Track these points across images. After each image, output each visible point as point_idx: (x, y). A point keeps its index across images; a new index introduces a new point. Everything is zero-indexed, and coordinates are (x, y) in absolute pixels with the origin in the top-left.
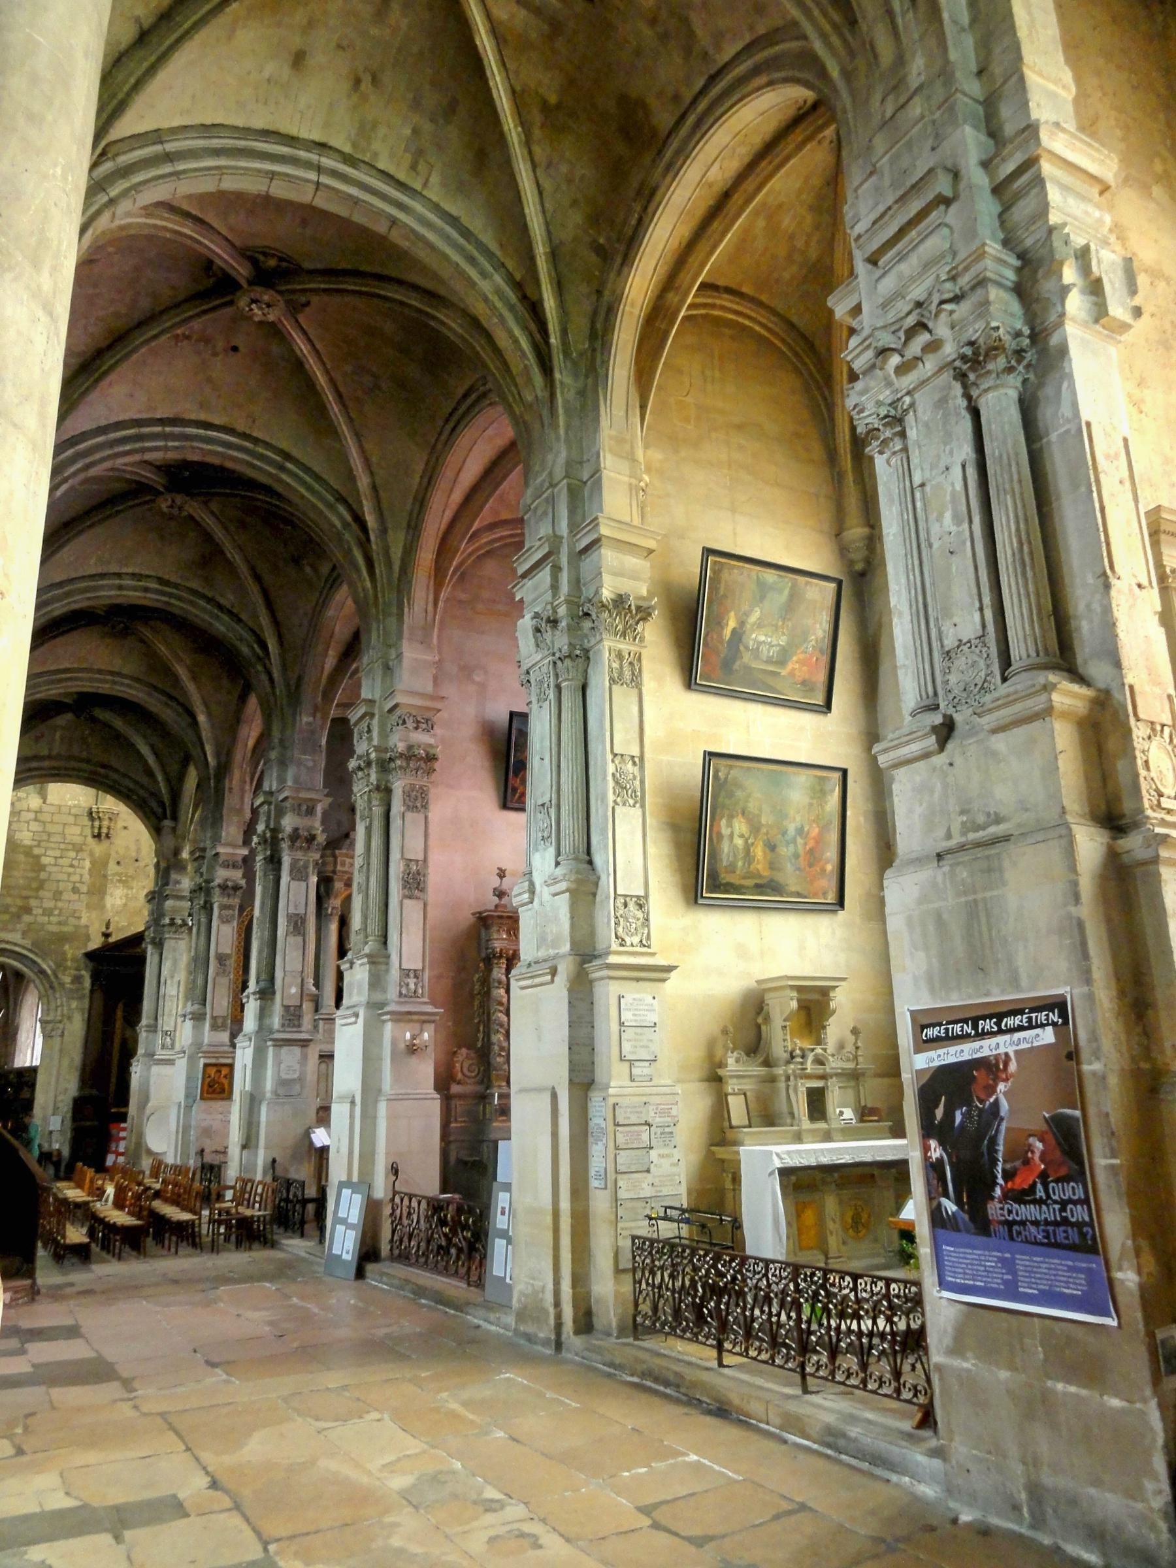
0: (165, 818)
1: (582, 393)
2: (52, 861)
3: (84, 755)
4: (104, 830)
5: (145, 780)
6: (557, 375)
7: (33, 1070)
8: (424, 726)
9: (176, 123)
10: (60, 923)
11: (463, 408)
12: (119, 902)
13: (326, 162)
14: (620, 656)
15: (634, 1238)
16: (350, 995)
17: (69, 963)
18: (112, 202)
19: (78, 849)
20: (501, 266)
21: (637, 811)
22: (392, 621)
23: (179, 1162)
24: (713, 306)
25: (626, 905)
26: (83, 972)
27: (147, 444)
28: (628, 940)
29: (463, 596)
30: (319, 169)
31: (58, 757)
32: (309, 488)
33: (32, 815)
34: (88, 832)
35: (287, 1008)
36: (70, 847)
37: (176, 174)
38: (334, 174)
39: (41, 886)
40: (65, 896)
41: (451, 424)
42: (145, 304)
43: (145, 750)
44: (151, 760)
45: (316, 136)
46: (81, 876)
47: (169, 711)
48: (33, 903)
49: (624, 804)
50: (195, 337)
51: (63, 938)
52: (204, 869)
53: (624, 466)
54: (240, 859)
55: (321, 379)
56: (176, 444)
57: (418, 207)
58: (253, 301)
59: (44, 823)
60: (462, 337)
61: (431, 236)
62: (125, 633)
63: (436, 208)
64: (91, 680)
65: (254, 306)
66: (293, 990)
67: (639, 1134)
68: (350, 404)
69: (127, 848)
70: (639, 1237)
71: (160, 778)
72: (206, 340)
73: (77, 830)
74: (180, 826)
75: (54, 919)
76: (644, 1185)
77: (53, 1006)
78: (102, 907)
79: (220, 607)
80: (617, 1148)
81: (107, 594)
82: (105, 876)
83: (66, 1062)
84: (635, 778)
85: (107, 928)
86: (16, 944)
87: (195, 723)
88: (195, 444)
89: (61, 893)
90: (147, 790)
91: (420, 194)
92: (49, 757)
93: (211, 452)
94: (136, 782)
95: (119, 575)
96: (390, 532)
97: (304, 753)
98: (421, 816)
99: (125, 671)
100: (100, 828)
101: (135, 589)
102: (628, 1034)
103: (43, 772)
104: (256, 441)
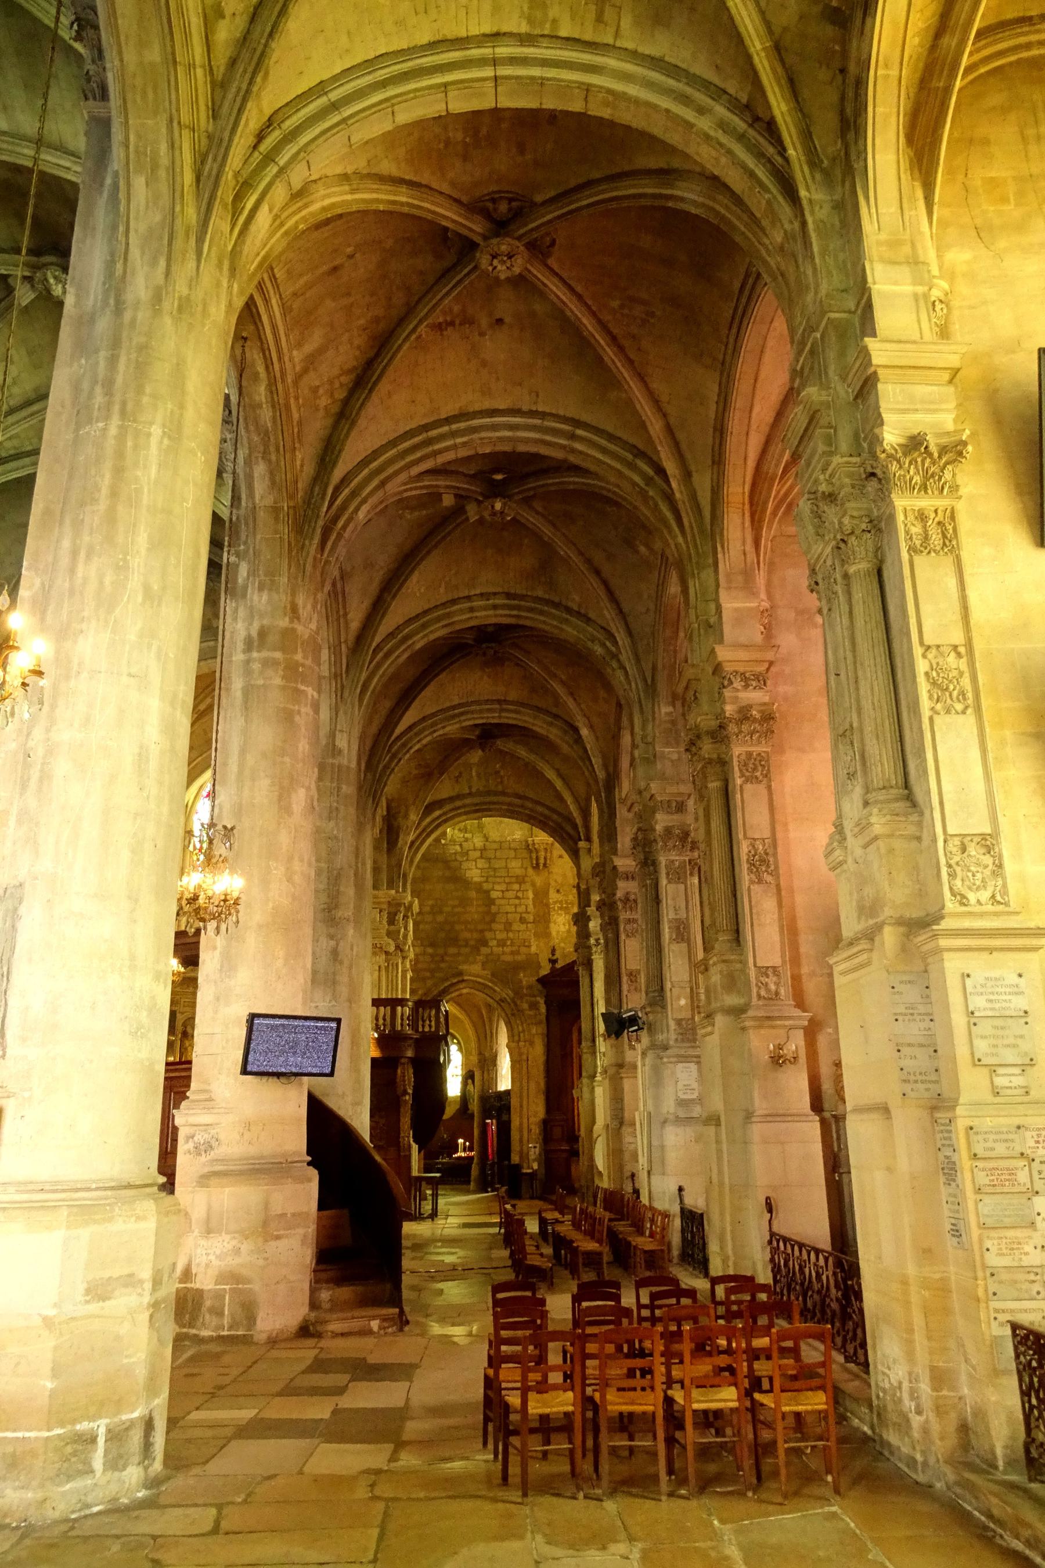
1: (839, 206)
2: (500, 894)
3: (500, 788)
4: (542, 861)
5: (556, 805)
6: (803, 193)
7: (507, 1093)
8: (754, 683)
9: (338, 70)
10: (512, 953)
11: (744, 300)
13: (502, 51)
14: (922, 516)
15: (1015, 1327)
18: (282, 170)
19: (521, 880)
20: (718, 93)
21: (970, 718)
22: (707, 574)
24: (1028, 46)
25: (964, 849)
27: (436, 447)
28: (972, 897)
30: (495, 62)
31: (479, 793)
32: (604, 450)
33: (478, 854)
34: (527, 863)
35: (679, 1022)
37: (344, 120)
38: (513, 61)
39: (493, 921)
40: (515, 927)
41: (734, 331)
42: (399, 299)
43: (550, 774)
44: (559, 784)
45: (487, 29)
48: (488, 935)
49: (948, 712)
50: (457, 322)
51: (517, 967)
52: (605, 884)
53: (904, 272)
55: (588, 323)
56: (464, 439)
57: (612, 62)
58: (494, 257)
60: (703, 205)
61: (633, 90)
62: (497, 661)
63: (634, 56)
64: (481, 711)
65: (495, 262)
66: (683, 1002)
67: (1012, 1172)
68: (626, 343)
69: (564, 876)
70: (1022, 1328)
71: (569, 800)
72: (468, 321)
75: (507, 950)
76: (1028, 1248)
77: (516, 1031)
78: (547, 935)
79: (568, 610)
80: (978, 1191)
81: (463, 619)
82: (547, 905)
84: (961, 674)
86: (478, 976)
87: (579, 740)
88: (483, 434)
89: (510, 924)
90: (559, 814)
91: (614, 46)
92: (470, 794)
93: (501, 439)
94: (548, 808)
95: (468, 598)
96: (695, 475)
97: (668, 744)
98: (762, 788)
99: (510, 698)
101: (485, 608)
102: (985, 1028)
104: (543, 415)
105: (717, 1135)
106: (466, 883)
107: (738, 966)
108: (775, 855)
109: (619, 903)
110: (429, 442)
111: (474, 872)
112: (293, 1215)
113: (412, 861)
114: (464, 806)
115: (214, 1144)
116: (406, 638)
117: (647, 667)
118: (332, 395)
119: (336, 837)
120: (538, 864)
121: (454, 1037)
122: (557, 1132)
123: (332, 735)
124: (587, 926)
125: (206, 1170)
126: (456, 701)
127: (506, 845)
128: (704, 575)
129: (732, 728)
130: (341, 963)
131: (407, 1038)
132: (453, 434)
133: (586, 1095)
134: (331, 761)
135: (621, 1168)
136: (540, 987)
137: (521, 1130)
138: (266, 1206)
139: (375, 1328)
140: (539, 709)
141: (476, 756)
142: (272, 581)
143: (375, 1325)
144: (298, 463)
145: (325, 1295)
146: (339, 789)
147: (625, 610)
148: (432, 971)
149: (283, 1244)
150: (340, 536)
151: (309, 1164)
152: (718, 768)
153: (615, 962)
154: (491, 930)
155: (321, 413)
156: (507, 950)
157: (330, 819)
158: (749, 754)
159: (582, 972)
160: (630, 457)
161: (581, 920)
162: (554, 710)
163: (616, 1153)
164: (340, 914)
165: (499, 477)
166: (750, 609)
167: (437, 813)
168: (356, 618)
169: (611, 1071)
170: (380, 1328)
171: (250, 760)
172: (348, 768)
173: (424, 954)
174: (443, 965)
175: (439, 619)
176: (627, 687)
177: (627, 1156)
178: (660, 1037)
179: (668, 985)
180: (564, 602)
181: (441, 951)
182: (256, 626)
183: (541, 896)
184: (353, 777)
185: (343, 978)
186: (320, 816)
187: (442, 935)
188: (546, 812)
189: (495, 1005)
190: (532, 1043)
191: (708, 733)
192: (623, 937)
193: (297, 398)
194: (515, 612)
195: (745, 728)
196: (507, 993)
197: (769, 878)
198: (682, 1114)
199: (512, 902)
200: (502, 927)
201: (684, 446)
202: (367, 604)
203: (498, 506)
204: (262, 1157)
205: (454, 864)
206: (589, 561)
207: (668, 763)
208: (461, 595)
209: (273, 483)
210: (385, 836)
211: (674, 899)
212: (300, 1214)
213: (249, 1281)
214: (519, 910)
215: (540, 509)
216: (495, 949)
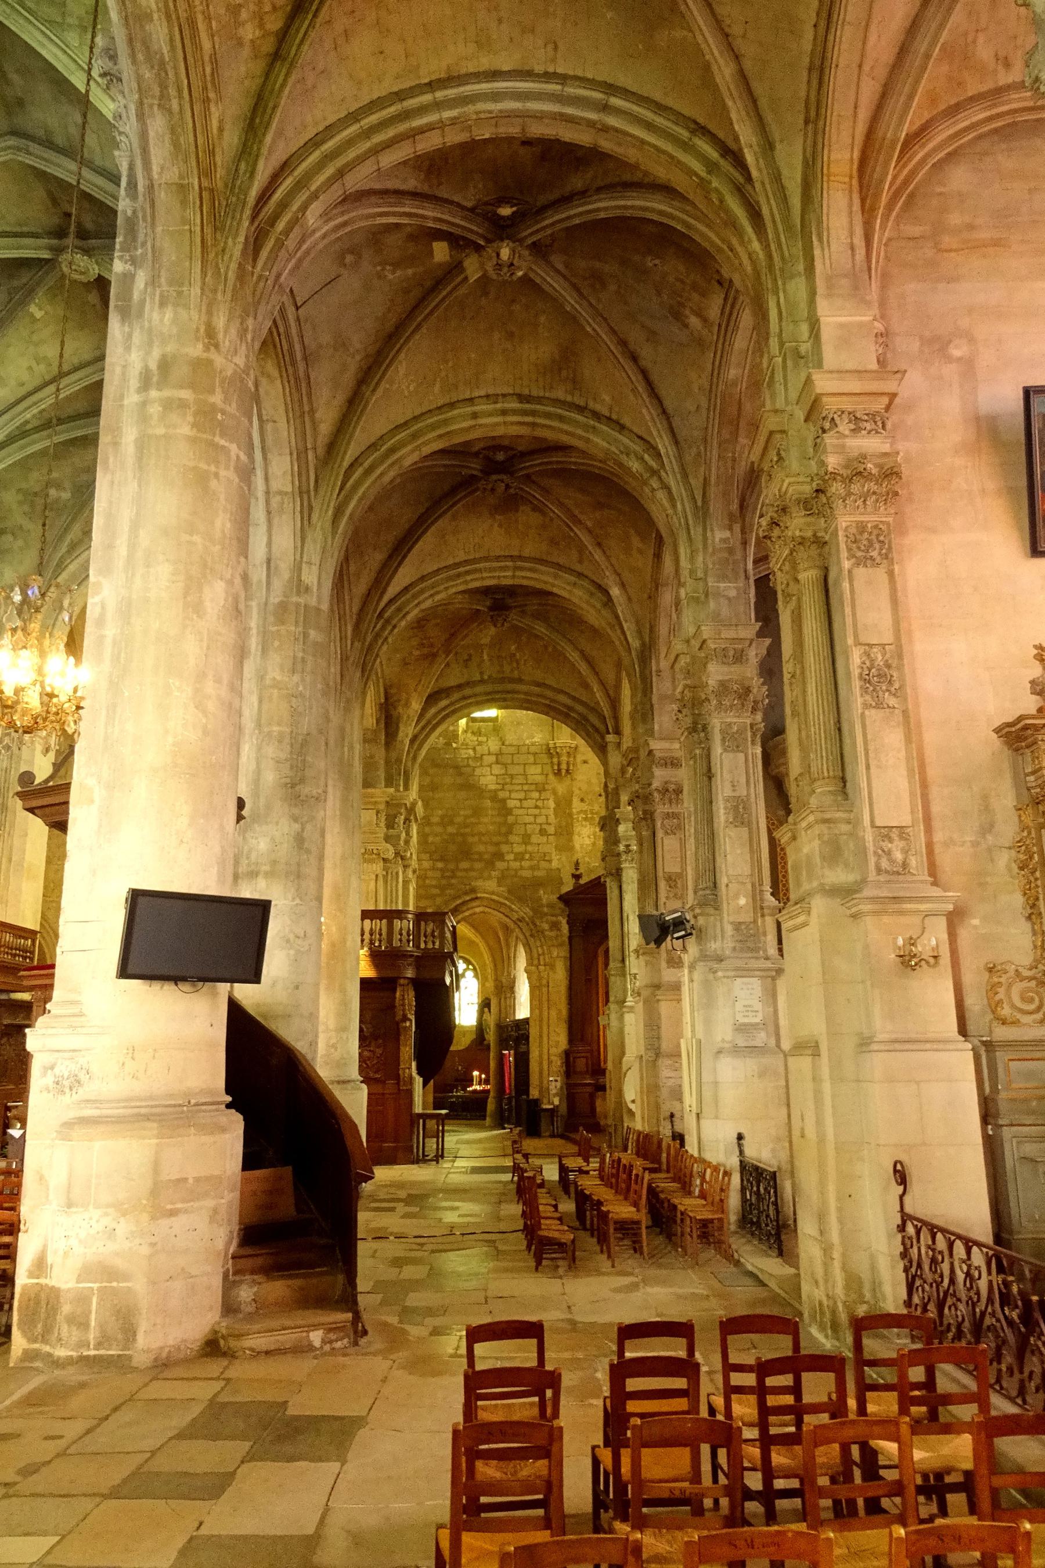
2: (518, 804)
3: (516, 674)
4: (564, 766)
7: (526, 1021)
10: (532, 868)
12: (587, 841)
16: (799, 884)
17: (545, 910)
19: (541, 788)
22: (798, 287)
23: (647, 1130)
26: (560, 918)
29: (916, 230)
31: (491, 680)
32: (649, 126)
33: (493, 759)
34: (548, 768)
35: (737, 926)
39: (510, 832)
40: (535, 839)
47: (578, 592)
48: (504, 848)
51: (537, 884)
62: (510, 503)
64: (491, 570)
66: (742, 901)
73: (538, 769)
75: (526, 864)
78: (569, 848)
79: (597, 416)
82: (570, 815)
83: (553, 1013)
86: (493, 893)
88: (481, 106)
89: (529, 836)
92: (482, 681)
94: (574, 698)
95: (471, 400)
96: (778, 146)
97: (723, 577)
98: (880, 574)
99: (526, 553)
103: (479, 699)
104: (563, 79)
105: (815, 1068)
107: (845, 828)
108: (900, 668)
109: (656, 794)
110: (406, 115)
111: (488, 778)
112: (197, 1180)
113: (415, 758)
115: (82, 1076)
116: (392, 450)
117: (696, 483)
118: (261, 26)
119: (301, 694)
120: (559, 770)
122: (581, 1064)
123: (297, 568)
124: (616, 831)
125: (73, 1114)
126: (461, 556)
127: (524, 749)
128: (791, 286)
129: (836, 488)
132: (438, 105)
133: (614, 1023)
136: (561, 905)
137: (541, 1063)
138: (156, 1167)
139: (317, 1343)
140: (559, 566)
141: (488, 633)
142: (180, 293)
143: (316, 1337)
144: (215, 124)
145: (245, 1293)
146: (306, 635)
147: (670, 410)
148: (443, 888)
149: (179, 1223)
150: (280, 244)
151: (229, 1106)
152: (814, 551)
153: (651, 863)
154: (507, 843)
155: (246, 52)
156: (526, 864)
157: (293, 671)
158: (862, 528)
159: (611, 886)
160: (684, 134)
161: (608, 824)
162: (578, 568)
163: (651, 1089)
164: (306, 790)
165: (506, 211)
166: (861, 325)
167: (444, 703)
168: (327, 417)
169: (645, 993)
170: (324, 1342)
171: (144, 538)
172: (318, 610)
173: (433, 869)
174: (453, 881)
175: (433, 427)
176: (670, 511)
177: (664, 1093)
178: (714, 946)
179: (723, 881)
180: (591, 405)
181: (452, 866)
182: (156, 353)
183: (563, 806)
184: (324, 622)
185: (311, 871)
186: (282, 669)
187: (453, 848)
188: (569, 702)
189: (512, 925)
190: (552, 967)
191: (798, 501)
192: (660, 834)
193: (208, 18)
194: (530, 419)
195: (855, 488)
196: (526, 912)
197: (892, 701)
198: (741, 1042)
199: (530, 811)
201: (763, 103)
202: (341, 398)
203: (505, 253)
204: (151, 1098)
205: (464, 770)
206: (623, 343)
207: (723, 602)
208: (461, 397)
209: (176, 144)
210: (383, 725)
211: (731, 772)
212: (208, 1179)
213: (126, 1277)
215: (560, 267)
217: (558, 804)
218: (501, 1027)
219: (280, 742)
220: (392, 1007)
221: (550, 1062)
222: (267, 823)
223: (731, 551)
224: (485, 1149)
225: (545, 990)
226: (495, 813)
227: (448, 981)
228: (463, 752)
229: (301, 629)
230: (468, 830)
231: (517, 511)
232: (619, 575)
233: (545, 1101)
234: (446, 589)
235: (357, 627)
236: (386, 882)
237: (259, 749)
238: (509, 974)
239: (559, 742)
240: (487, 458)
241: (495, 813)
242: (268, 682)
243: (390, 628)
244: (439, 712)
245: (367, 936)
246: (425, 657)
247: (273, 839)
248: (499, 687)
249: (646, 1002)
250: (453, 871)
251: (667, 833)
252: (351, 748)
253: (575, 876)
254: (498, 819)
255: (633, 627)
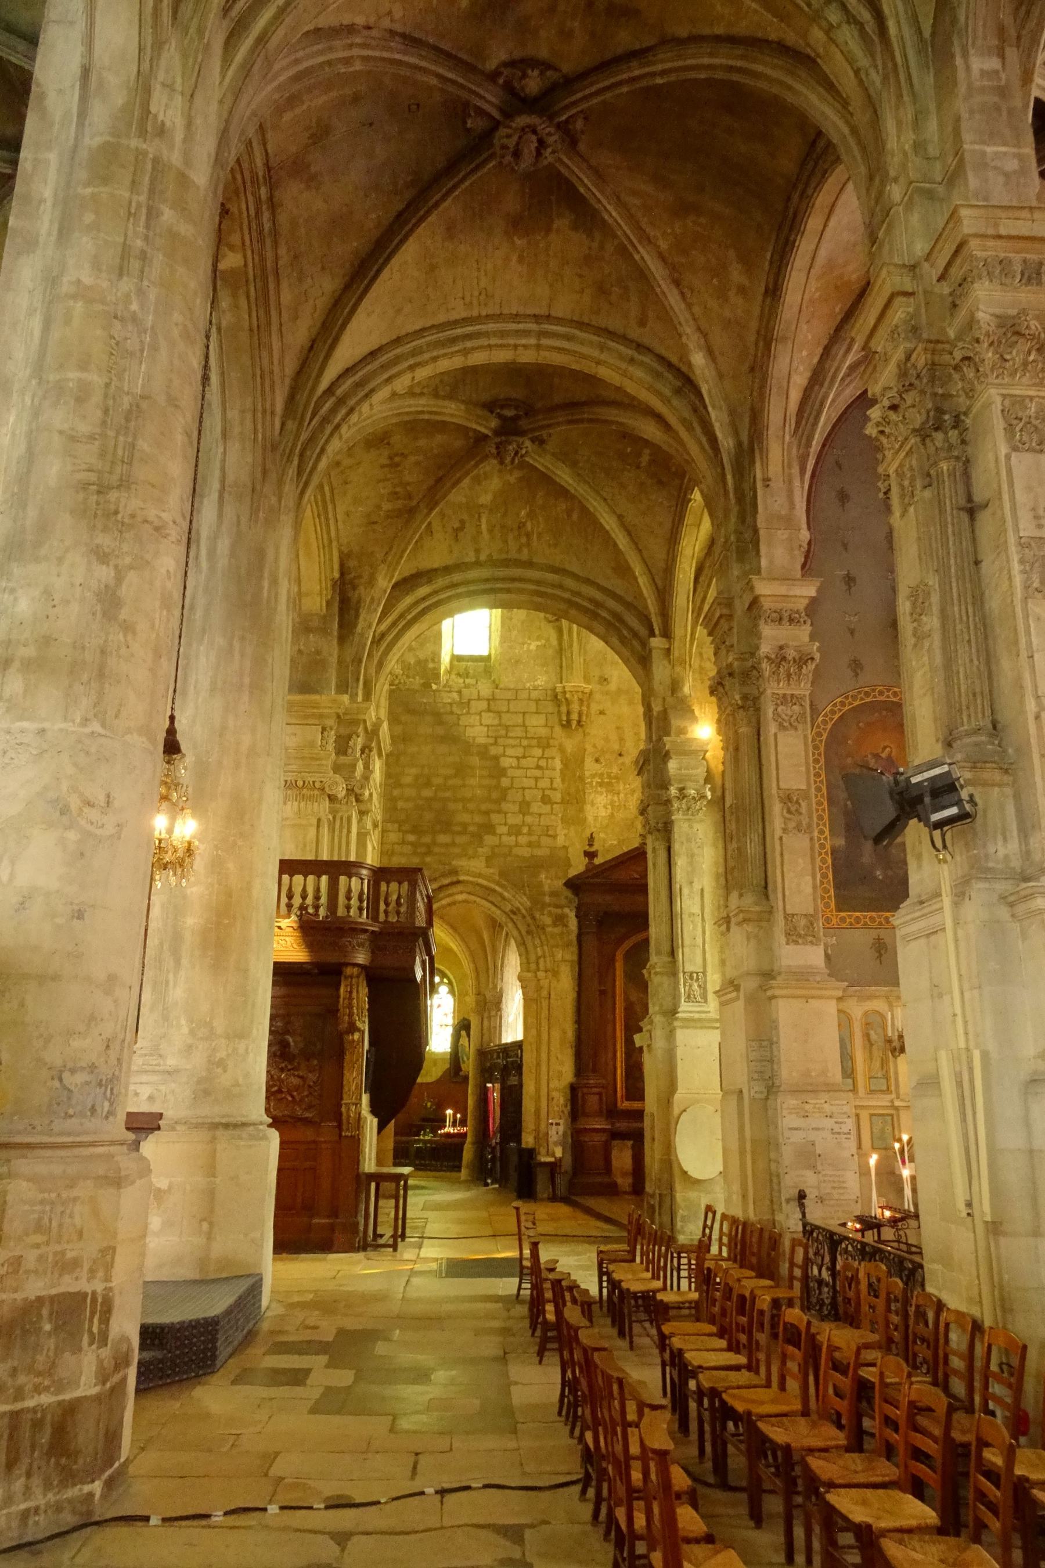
0: (652, 634)
2: (514, 762)
3: (525, 555)
4: (575, 717)
5: (616, 584)
7: (518, 1045)
10: (530, 845)
12: (603, 813)
17: (547, 899)
19: (544, 744)
26: (567, 910)
33: (484, 705)
36: (534, 742)
39: (504, 798)
40: (535, 808)
43: (609, 522)
44: (622, 541)
46: (552, 780)
47: (639, 373)
48: (495, 818)
51: (536, 865)
54: (801, 605)
59: (499, 713)
64: (502, 334)
69: (607, 740)
71: (638, 569)
74: (676, 644)
75: (523, 840)
77: (533, 958)
78: (582, 822)
82: (581, 779)
83: (556, 1034)
85: (591, 845)
86: (480, 875)
89: (528, 804)
92: (478, 564)
97: (992, 136)
99: (558, 312)
100: (568, 713)
103: (472, 588)
106: (467, 747)
109: (765, 665)
114: (466, 583)
119: (134, 318)
120: (569, 721)
121: (443, 975)
122: (593, 1102)
123: (143, 86)
127: (524, 695)
130: (128, 628)
131: (355, 929)
133: (659, 1043)
134: (134, 143)
135: (771, 1180)
136: (569, 893)
137: (538, 1099)
146: (152, 214)
153: (755, 778)
154: (499, 812)
156: (523, 840)
164: (130, 503)
167: (423, 591)
172: (183, 181)
173: (403, 842)
177: (787, 1154)
181: (427, 839)
183: (573, 765)
186: (96, 265)
187: (429, 816)
188: (598, 596)
190: (556, 974)
192: (771, 728)
196: (522, 902)
200: (516, 808)
211: (1029, 489)
214: (542, 784)
216: (505, 839)
217: (566, 764)
218: (483, 1054)
219: (80, 400)
220: (332, 1011)
221: (550, 1099)
222: (37, 560)
223: (1003, 92)
224: (460, 1222)
225: (545, 1004)
226: (485, 773)
227: (419, 974)
228: (443, 694)
229: (143, 198)
230: (448, 794)
231: (548, 230)
232: (705, 336)
233: (543, 1151)
234: (435, 359)
235: (291, 399)
236: (332, 830)
237: (36, 413)
238: (495, 986)
239: (569, 686)
240: (509, 88)
241: (485, 773)
242: (66, 287)
243: (343, 411)
244: (416, 603)
245: (297, 901)
246: (398, 514)
247: (48, 593)
248: (501, 573)
249: (751, 999)
250: (428, 846)
251: (781, 727)
252: (274, 582)
253: (587, 854)
254: (486, 782)
255: (725, 417)
